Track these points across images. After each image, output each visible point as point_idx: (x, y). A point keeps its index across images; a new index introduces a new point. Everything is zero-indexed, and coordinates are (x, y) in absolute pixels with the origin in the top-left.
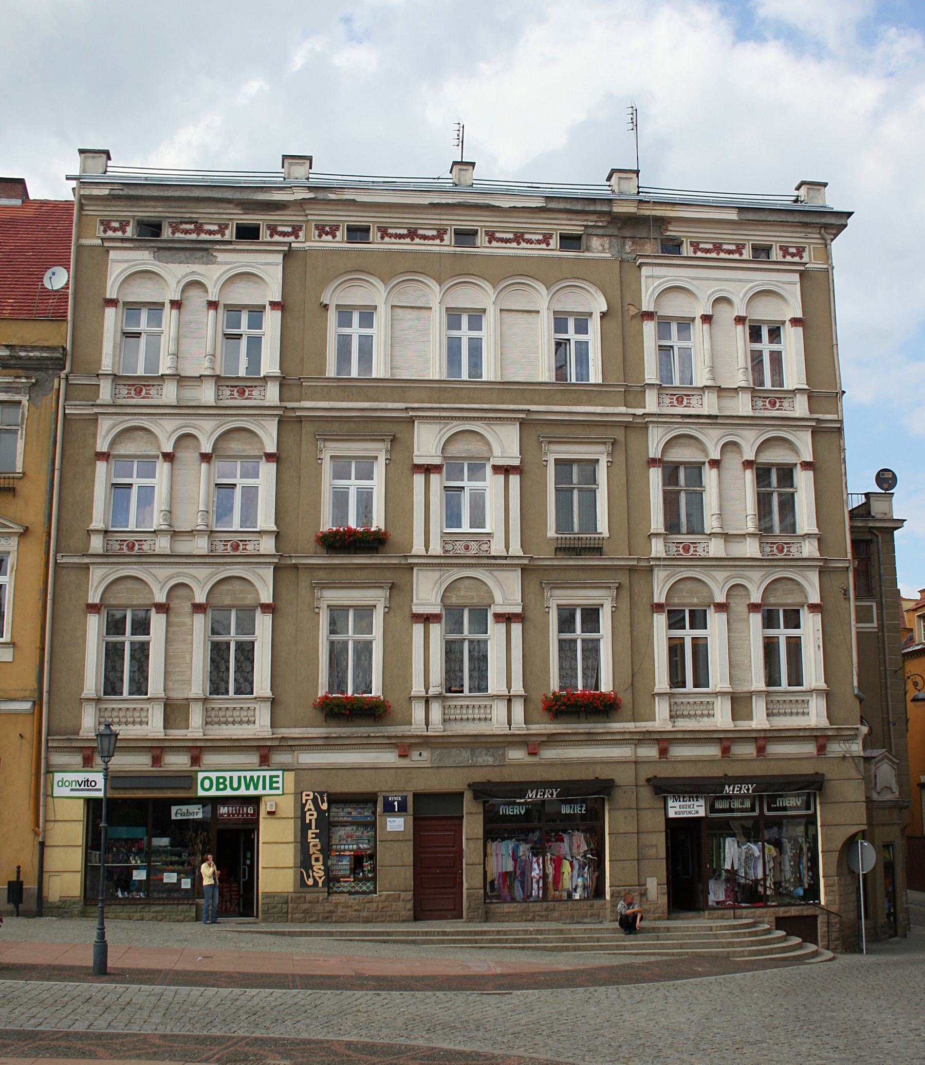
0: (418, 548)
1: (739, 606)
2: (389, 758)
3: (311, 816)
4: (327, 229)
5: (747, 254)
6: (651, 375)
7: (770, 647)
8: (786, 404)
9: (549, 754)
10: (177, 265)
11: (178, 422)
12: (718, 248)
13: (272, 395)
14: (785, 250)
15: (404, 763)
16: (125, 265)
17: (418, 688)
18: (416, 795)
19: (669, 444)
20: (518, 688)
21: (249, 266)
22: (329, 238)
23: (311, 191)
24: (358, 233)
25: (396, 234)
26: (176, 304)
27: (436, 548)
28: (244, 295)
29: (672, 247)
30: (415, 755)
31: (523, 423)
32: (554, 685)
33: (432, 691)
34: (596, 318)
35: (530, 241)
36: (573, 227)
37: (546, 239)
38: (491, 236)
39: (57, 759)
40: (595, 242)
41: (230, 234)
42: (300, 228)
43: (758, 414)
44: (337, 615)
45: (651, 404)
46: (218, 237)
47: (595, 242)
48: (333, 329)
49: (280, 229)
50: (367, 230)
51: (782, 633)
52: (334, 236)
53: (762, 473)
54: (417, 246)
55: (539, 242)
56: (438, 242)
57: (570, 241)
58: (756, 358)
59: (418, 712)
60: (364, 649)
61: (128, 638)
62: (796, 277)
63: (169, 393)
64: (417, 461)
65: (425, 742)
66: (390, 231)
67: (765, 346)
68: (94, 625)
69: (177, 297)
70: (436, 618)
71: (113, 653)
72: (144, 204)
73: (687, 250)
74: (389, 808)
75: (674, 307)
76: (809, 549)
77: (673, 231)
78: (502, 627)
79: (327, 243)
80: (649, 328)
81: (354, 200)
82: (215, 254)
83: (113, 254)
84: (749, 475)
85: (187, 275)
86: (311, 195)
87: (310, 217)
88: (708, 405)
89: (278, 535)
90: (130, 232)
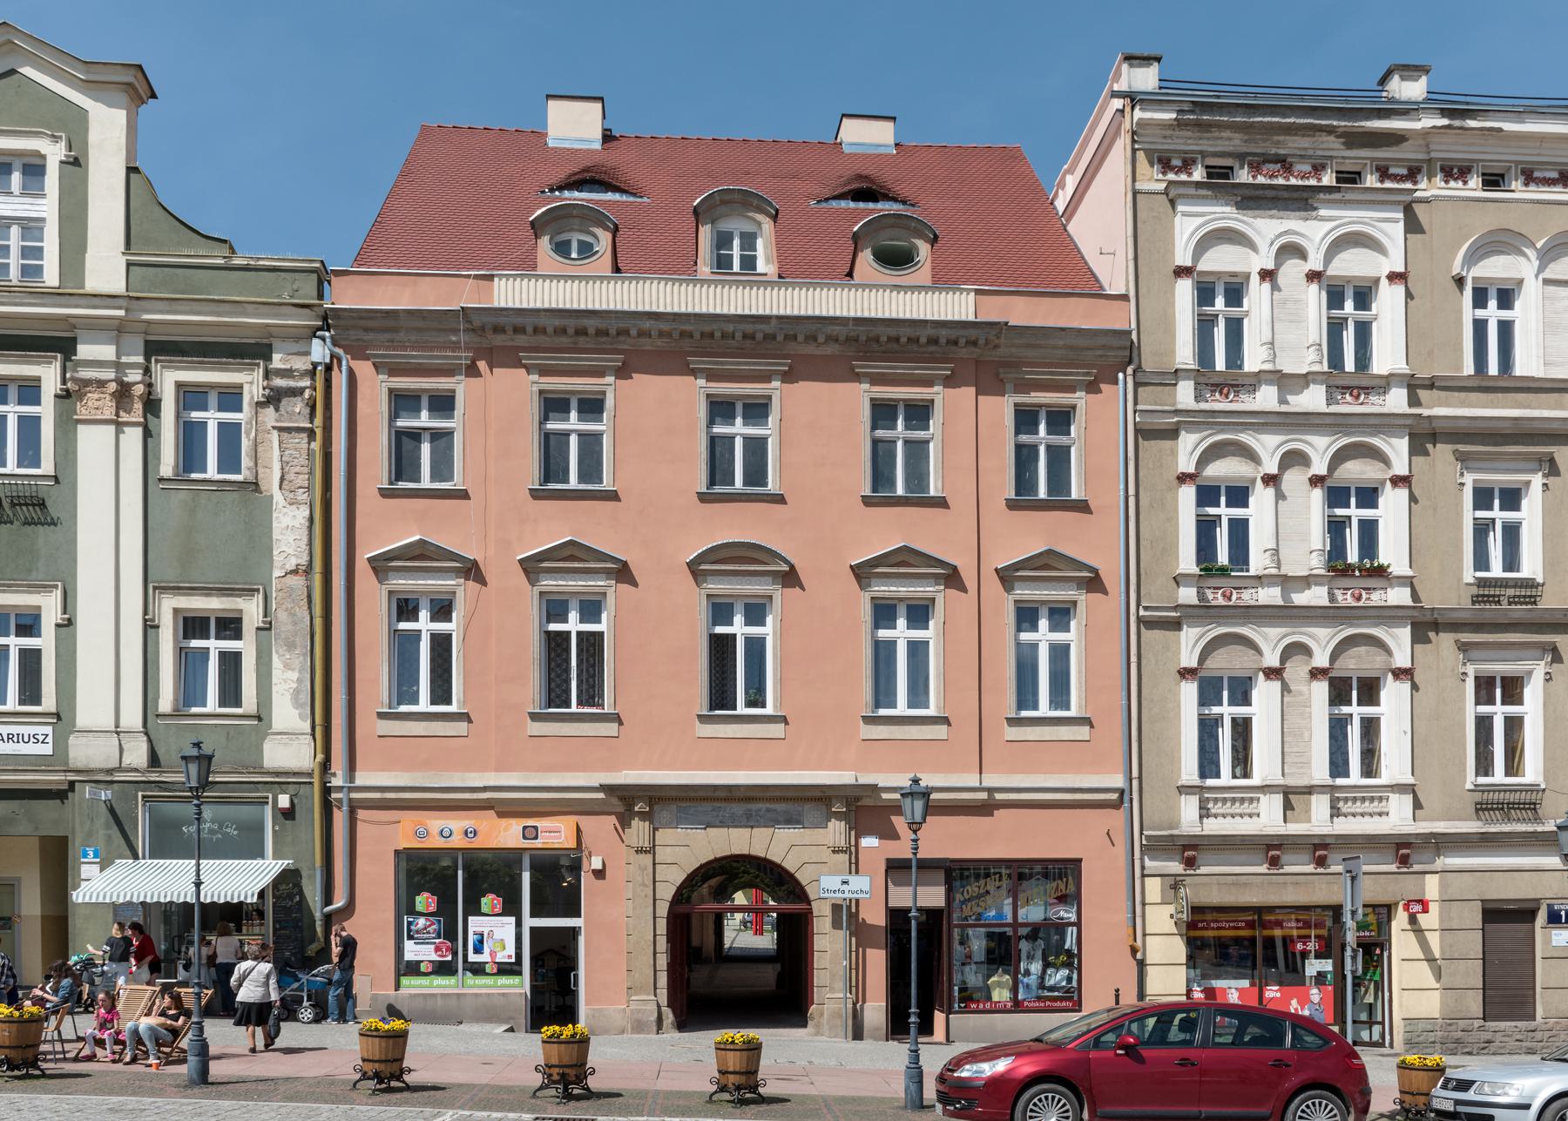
4: (1455, 170)
10: (1267, 220)
11: (1278, 439)
16: (1200, 220)
21: (1361, 223)
22: (1460, 184)
23: (1443, 117)
25: (1544, 178)
26: (1267, 275)
28: (1351, 264)
41: (1328, 179)
42: (1419, 170)
46: (1313, 182)
49: (1392, 171)
52: (1465, 183)
66: (1536, 174)
69: (1270, 266)
72: (1217, 134)
79: (1455, 189)
81: (1500, 130)
82: (1315, 205)
85: (1281, 235)
86: (1445, 122)
87: (1433, 155)
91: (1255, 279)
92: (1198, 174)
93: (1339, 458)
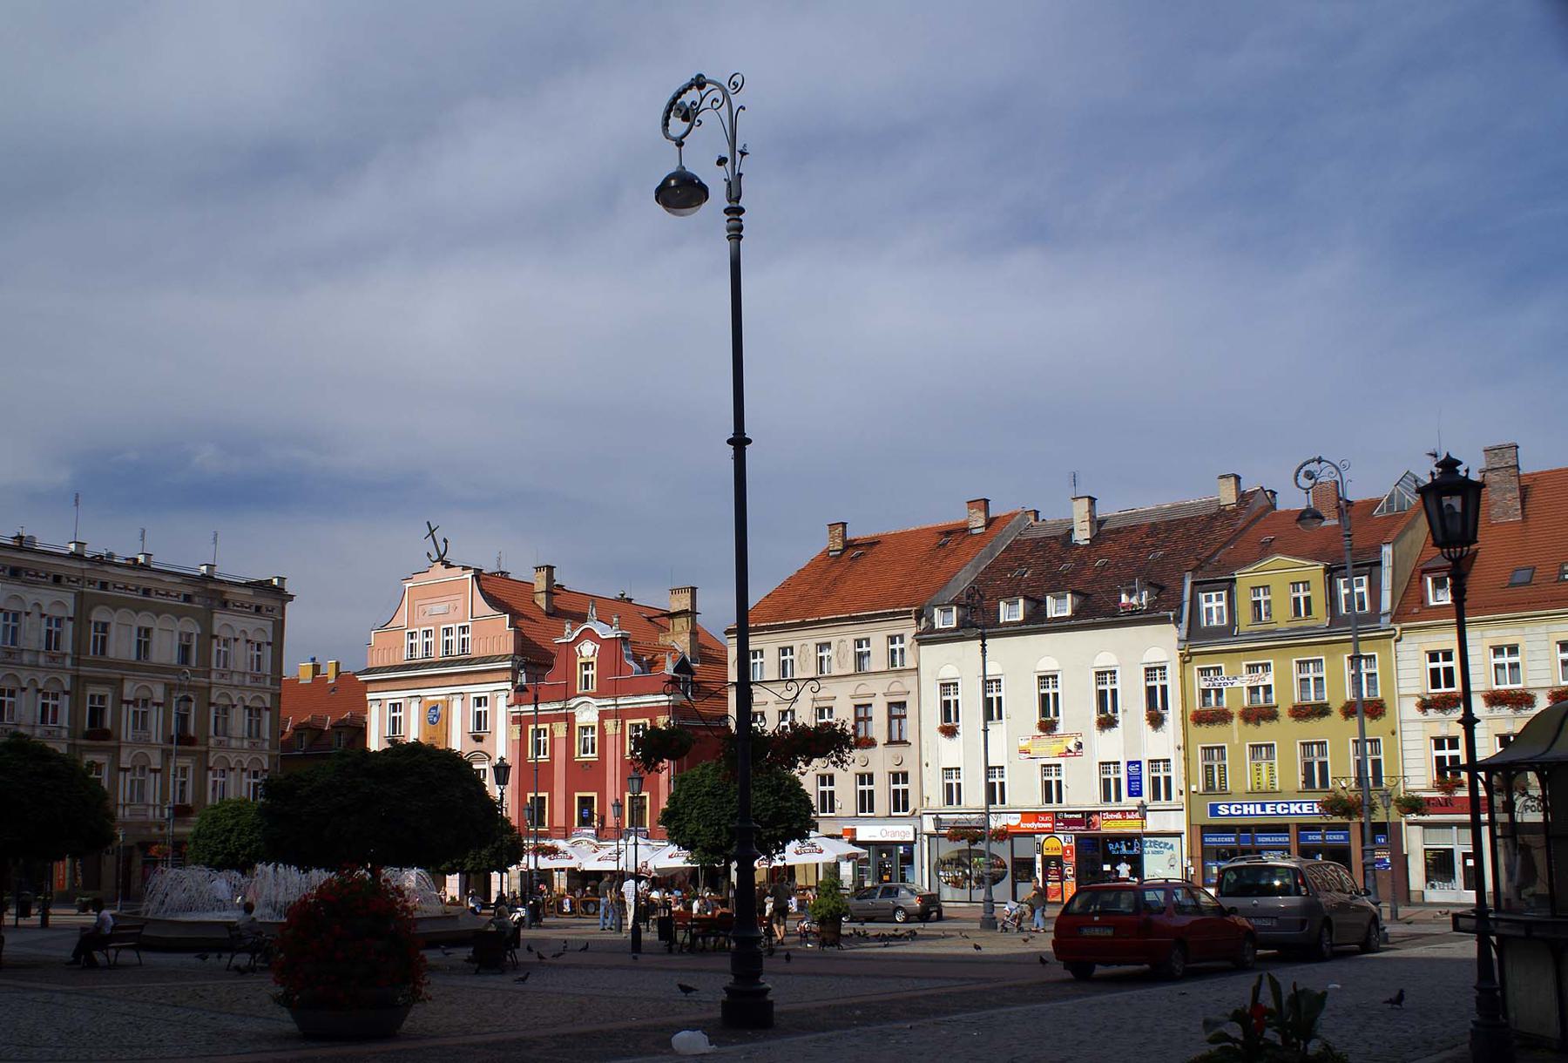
0: (123, 738)
6: (214, 666)
8: (262, 680)
12: (242, 606)
13: (68, 662)
14: (267, 610)
17: (121, 801)
19: (219, 696)
24: (104, 586)
29: (225, 604)
31: (166, 684)
33: (127, 802)
34: (195, 636)
35: (171, 596)
36: (188, 590)
38: (157, 593)
40: (196, 599)
47: (196, 599)
48: (92, 634)
55: (175, 597)
56: (135, 593)
57: (188, 598)
59: (120, 812)
62: (271, 623)
63: (26, 658)
64: (125, 698)
75: (226, 634)
76: (267, 745)
77: (227, 597)
78: (152, 775)
80: (215, 641)
88: (236, 679)
91: (23, 614)
92: (7, 572)
93: (48, 681)
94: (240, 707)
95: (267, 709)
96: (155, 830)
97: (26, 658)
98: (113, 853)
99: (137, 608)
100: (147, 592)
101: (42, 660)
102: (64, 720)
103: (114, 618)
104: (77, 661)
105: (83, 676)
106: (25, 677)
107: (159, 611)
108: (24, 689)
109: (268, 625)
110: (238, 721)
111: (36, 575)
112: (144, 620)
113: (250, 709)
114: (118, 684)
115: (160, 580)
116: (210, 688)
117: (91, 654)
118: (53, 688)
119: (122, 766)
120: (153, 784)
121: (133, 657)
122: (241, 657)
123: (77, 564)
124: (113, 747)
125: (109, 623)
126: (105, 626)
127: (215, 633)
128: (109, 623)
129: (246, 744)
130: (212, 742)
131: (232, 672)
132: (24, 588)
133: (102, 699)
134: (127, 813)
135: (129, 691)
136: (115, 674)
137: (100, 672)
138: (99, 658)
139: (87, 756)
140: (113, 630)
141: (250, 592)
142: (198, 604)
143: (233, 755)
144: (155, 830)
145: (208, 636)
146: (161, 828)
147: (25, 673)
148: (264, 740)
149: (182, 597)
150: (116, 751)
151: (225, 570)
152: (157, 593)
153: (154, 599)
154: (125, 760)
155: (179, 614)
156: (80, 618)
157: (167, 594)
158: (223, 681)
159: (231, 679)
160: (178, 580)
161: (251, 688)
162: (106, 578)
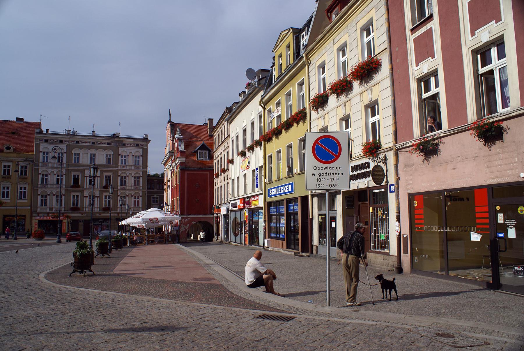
1: (130, 196)
2: (80, 215)
3: (70, 223)
5: (135, 145)
6: (120, 163)
7: (135, 201)
9: (102, 215)
12: (131, 145)
14: (141, 145)
15: (82, 216)
17: (85, 206)
18: (84, 220)
19: (121, 173)
20: (98, 206)
24: (77, 142)
27: (88, 187)
29: (124, 145)
30: (84, 215)
32: (104, 206)
34: (112, 155)
36: (109, 141)
37: (105, 143)
38: (97, 143)
39: (34, 215)
40: (113, 144)
43: (135, 169)
44: (74, 196)
45: (119, 168)
47: (113, 144)
50: (79, 141)
51: (136, 199)
53: (135, 177)
54: (86, 144)
57: (109, 144)
58: (136, 160)
59: (84, 209)
60: (77, 201)
61: (44, 199)
62: (142, 149)
63: (50, 165)
65: (85, 213)
67: (137, 159)
68: (39, 197)
70: (87, 197)
71: (42, 201)
73: (126, 145)
74: (80, 221)
75: (124, 154)
76: (141, 188)
77: (124, 142)
78: (96, 198)
79: (73, 144)
83: (41, 145)
84: (133, 178)
88: (128, 168)
89: (65, 185)
90: (43, 141)
94: (130, 176)
95: (141, 176)
96: (98, 215)
97: (50, 165)
98: (82, 222)
99: (89, 148)
100: (93, 143)
101: (55, 165)
102: (64, 183)
103: (81, 152)
104: (68, 164)
105: (70, 169)
106: (49, 171)
107: (97, 148)
108: (49, 174)
109: (141, 150)
110: (130, 181)
111: (54, 141)
112: (93, 151)
113: (135, 177)
114: (83, 171)
115: (96, 139)
116: (118, 171)
117: (73, 162)
118: (59, 174)
119: (85, 196)
120: (97, 201)
121: (89, 163)
122: (130, 161)
123: (69, 137)
124: (81, 190)
125: (79, 153)
126: (79, 154)
127: (120, 154)
128: (79, 153)
129: (133, 188)
130: (119, 187)
131: (127, 165)
132: (49, 145)
133: (78, 176)
134: (87, 209)
135: (87, 173)
136: (81, 168)
137: (76, 168)
138: (77, 163)
139: (72, 193)
140: (81, 155)
141: (132, 140)
142: (113, 145)
143: (127, 191)
144: (98, 215)
145: (117, 154)
146: (100, 214)
147: (49, 170)
148: (140, 186)
149: (107, 144)
150: (82, 192)
151: (123, 134)
152: (97, 143)
153: (96, 145)
154: (86, 193)
155: (105, 149)
156: (69, 152)
157: (101, 143)
158: (123, 168)
159: (127, 167)
160: (103, 138)
161: (133, 170)
162: (78, 140)
